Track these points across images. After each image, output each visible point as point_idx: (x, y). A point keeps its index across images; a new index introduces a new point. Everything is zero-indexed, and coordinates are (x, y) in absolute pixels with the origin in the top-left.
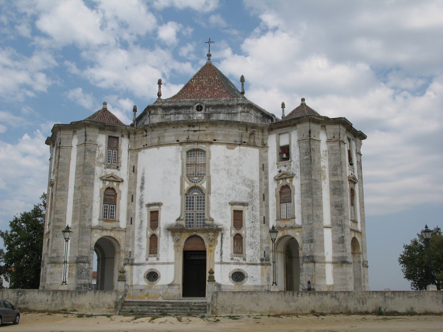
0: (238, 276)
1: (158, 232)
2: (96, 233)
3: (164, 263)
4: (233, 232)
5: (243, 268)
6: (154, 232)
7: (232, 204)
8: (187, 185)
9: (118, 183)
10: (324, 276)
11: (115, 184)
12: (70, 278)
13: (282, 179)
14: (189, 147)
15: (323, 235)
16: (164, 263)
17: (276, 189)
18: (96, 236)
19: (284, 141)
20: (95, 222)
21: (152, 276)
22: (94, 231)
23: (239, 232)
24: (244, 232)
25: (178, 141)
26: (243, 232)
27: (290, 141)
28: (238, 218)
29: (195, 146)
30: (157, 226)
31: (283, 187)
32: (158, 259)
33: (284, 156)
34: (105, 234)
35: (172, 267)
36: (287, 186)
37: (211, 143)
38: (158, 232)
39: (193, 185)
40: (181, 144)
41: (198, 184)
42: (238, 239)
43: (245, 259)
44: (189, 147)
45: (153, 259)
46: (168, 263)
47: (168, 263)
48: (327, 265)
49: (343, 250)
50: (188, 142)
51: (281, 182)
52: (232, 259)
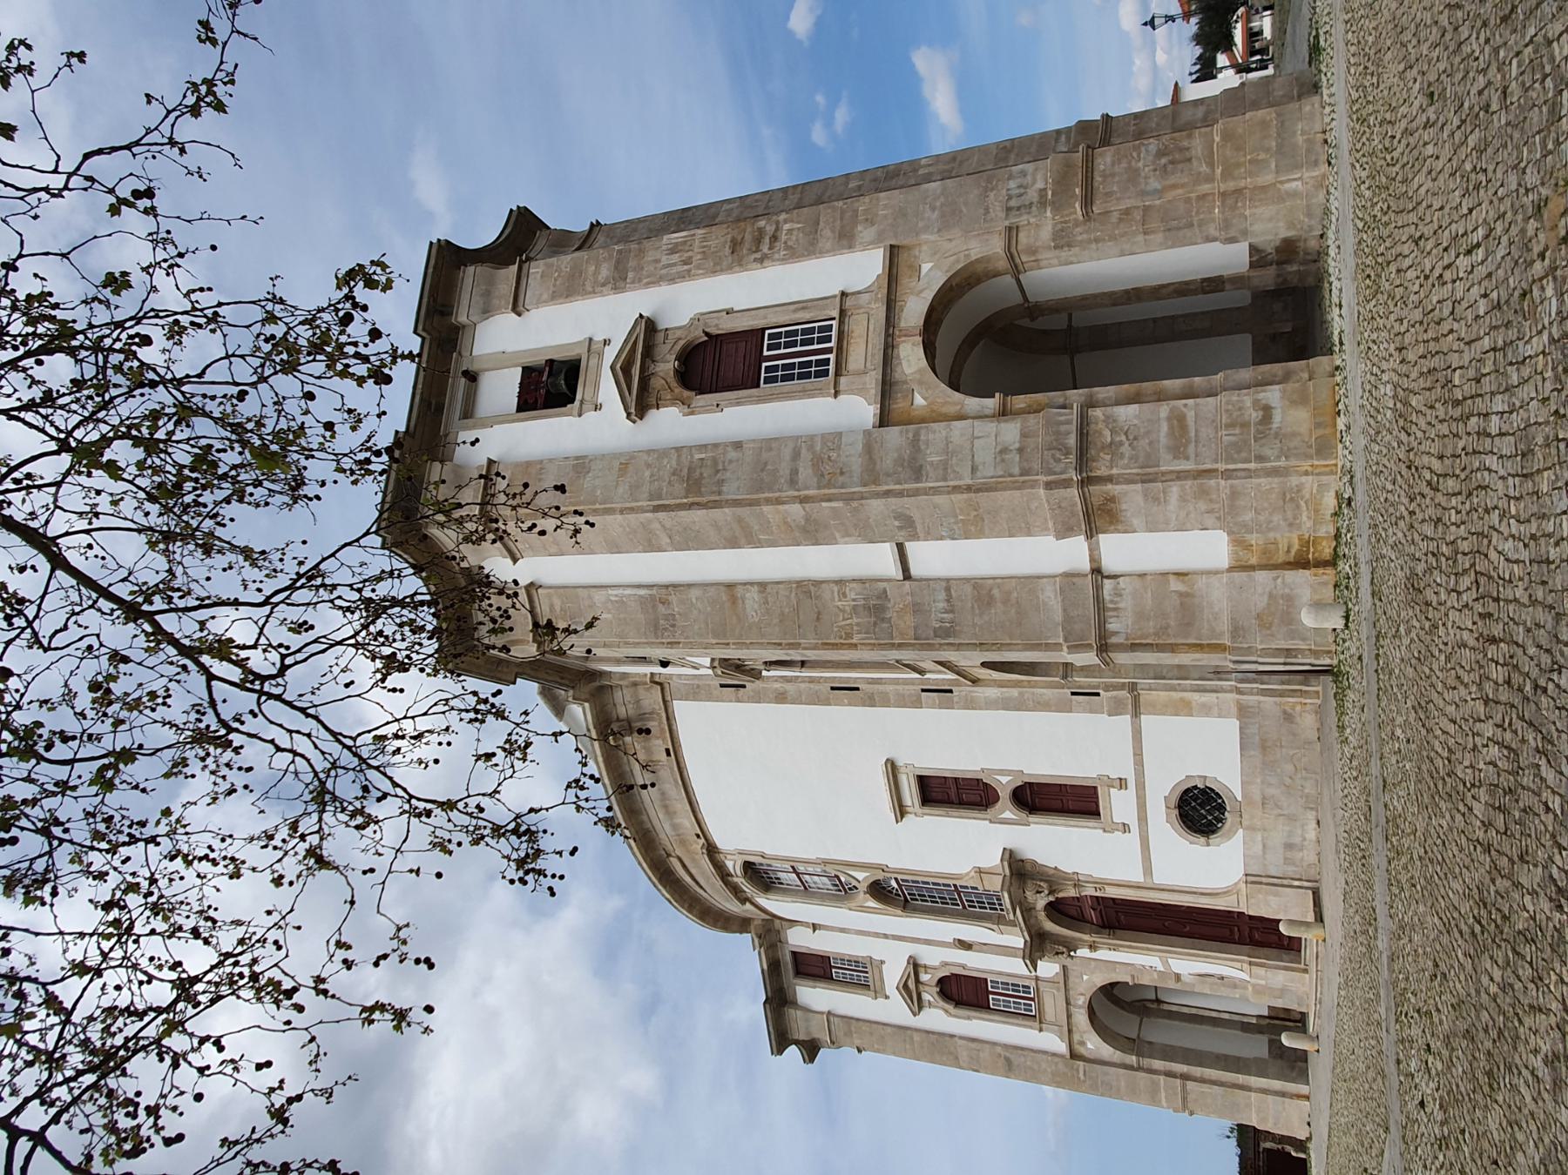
0: (1200, 810)
2: (1083, 1043)
4: (1008, 815)
5: (1163, 786)
7: (901, 811)
8: (872, 903)
9: (921, 970)
10: (1175, 585)
11: (924, 977)
14: (748, 888)
15: (948, 583)
18: (1093, 1044)
22: (1081, 1050)
23: (1005, 795)
24: (1004, 779)
26: (1004, 784)
28: (948, 793)
34: (1081, 1018)
37: (711, 850)
42: (1039, 799)
43: (1122, 783)
44: (748, 888)
48: (1109, 563)
52: (1125, 828)
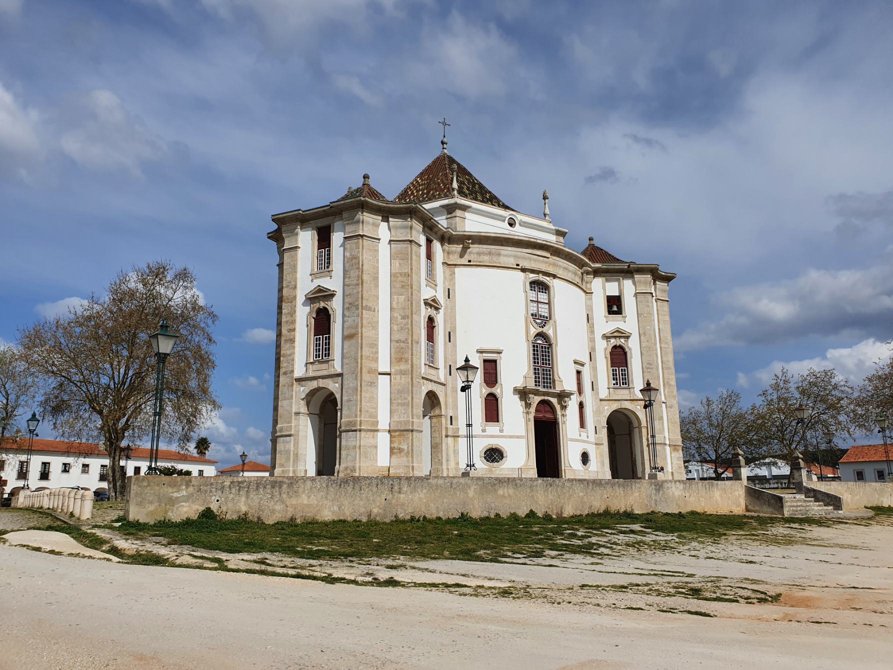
1: (499, 391)
3: (511, 437)
6: (493, 390)
8: (533, 331)
12: (394, 456)
13: (615, 337)
14: (533, 277)
16: (511, 437)
17: (605, 349)
19: (612, 289)
20: (423, 370)
21: (494, 455)
25: (518, 265)
27: (620, 291)
29: (541, 278)
30: (496, 382)
31: (615, 347)
32: (501, 431)
33: (615, 308)
35: (523, 442)
36: (620, 347)
38: (499, 391)
39: (540, 330)
40: (524, 270)
41: (545, 330)
44: (533, 277)
45: (493, 429)
46: (518, 437)
47: (518, 437)
49: (665, 429)
50: (533, 271)
51: (613, 340)
